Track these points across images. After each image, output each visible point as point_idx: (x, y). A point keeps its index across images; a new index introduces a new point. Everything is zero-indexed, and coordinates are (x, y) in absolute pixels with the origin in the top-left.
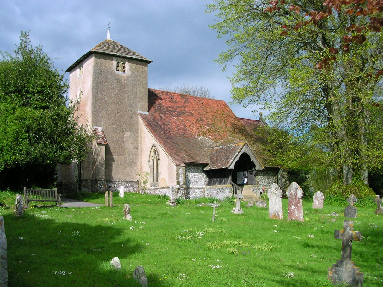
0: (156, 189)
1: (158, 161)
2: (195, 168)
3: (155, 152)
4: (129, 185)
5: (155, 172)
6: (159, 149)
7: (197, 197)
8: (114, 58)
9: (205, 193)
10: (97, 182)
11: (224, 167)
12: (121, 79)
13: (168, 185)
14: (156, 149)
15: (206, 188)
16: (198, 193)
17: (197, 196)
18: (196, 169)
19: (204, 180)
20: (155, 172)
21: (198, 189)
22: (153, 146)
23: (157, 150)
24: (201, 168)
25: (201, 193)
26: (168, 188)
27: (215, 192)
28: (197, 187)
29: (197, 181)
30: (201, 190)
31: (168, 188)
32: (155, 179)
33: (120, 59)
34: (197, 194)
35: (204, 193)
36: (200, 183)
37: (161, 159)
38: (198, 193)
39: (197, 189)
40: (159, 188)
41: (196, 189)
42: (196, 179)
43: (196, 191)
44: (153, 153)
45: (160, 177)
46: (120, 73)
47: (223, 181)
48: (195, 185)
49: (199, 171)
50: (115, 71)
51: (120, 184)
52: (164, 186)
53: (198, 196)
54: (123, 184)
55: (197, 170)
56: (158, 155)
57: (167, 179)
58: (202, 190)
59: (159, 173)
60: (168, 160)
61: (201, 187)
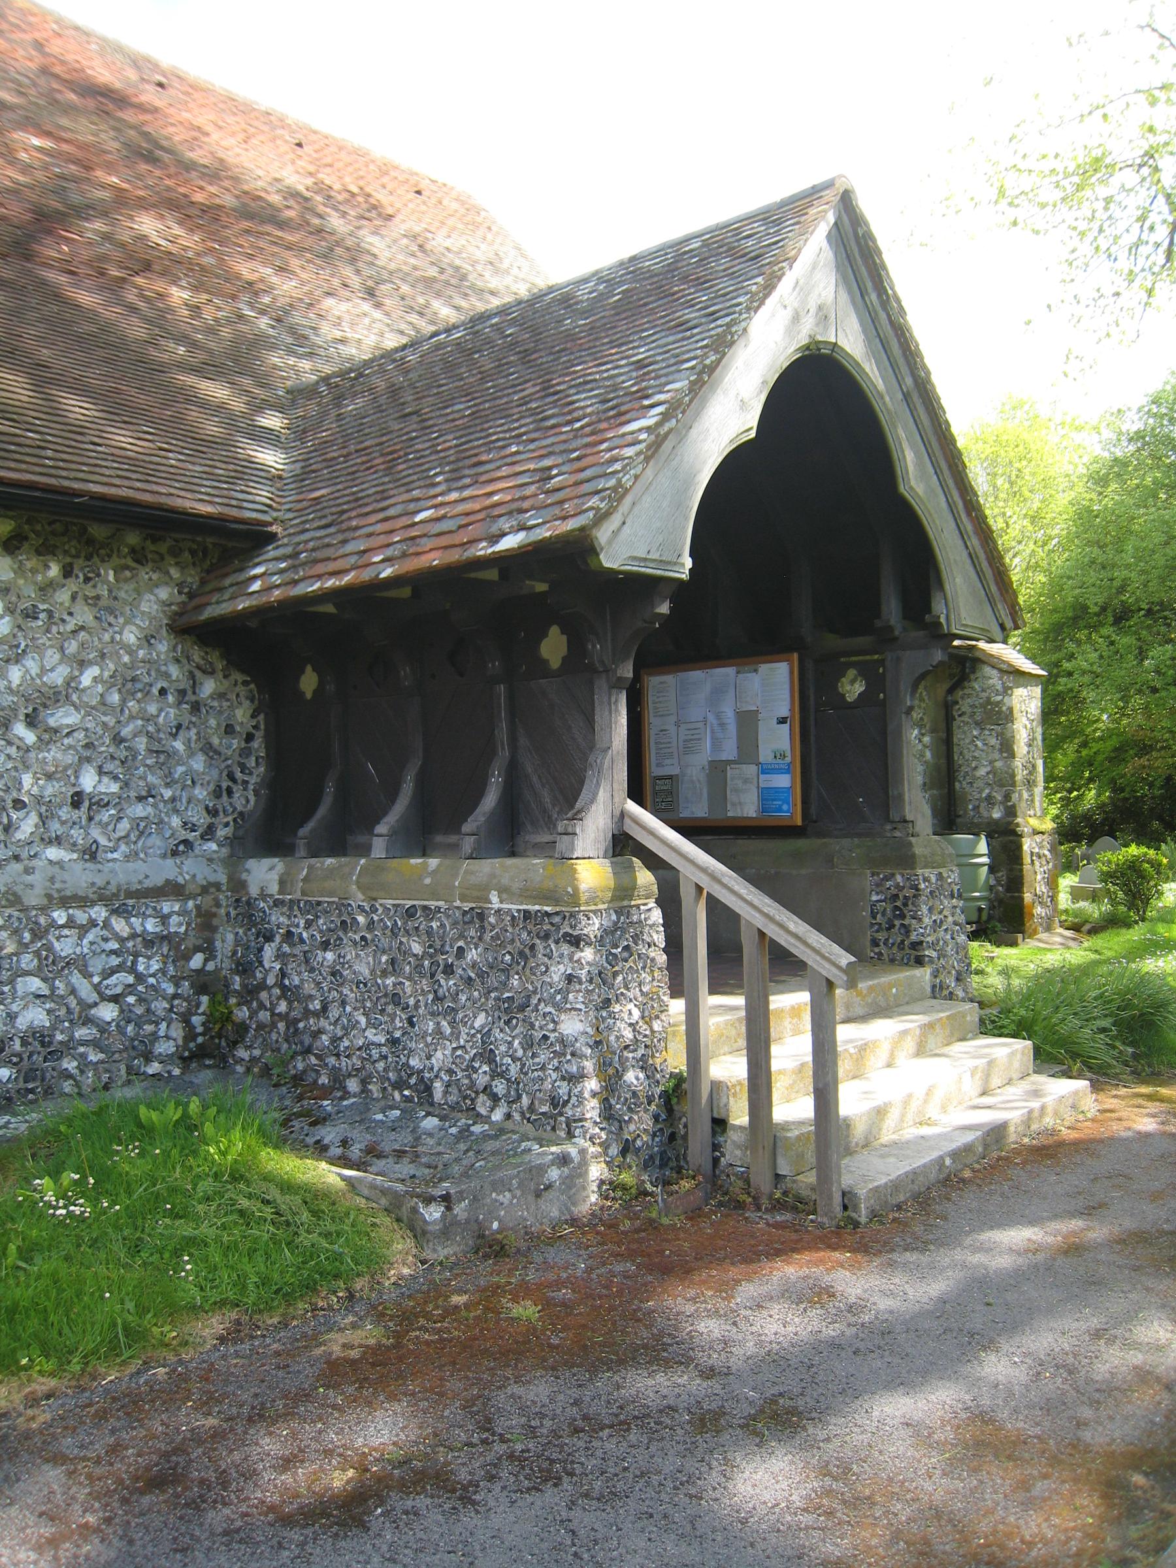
2: (46, 589)
7: (81, 1033)
9: (210, 953)
11: (510, 542)
15: (238, 885)
16: (97, 965)
17: (88, 1021)
18: (63, 596)
19: (198, 763)
21: (99, 913)
25: (150, 965)
27: (363, 970)
28: (81, 877)
29: (88, 781)
30: (151, 926)
34: (85, 990)
35: (197, 961)
36: (139, 810)
38: (97, 965)
39: (84, 902)
41: (60, 916)
42: (53, 755)
43: (65, 947)
47: (490, 800)
48: (53, 853)
49: (130, 637)
53: (108, 1012)
55: (84, 615)
58: (177, 925)
61: (167, 870)
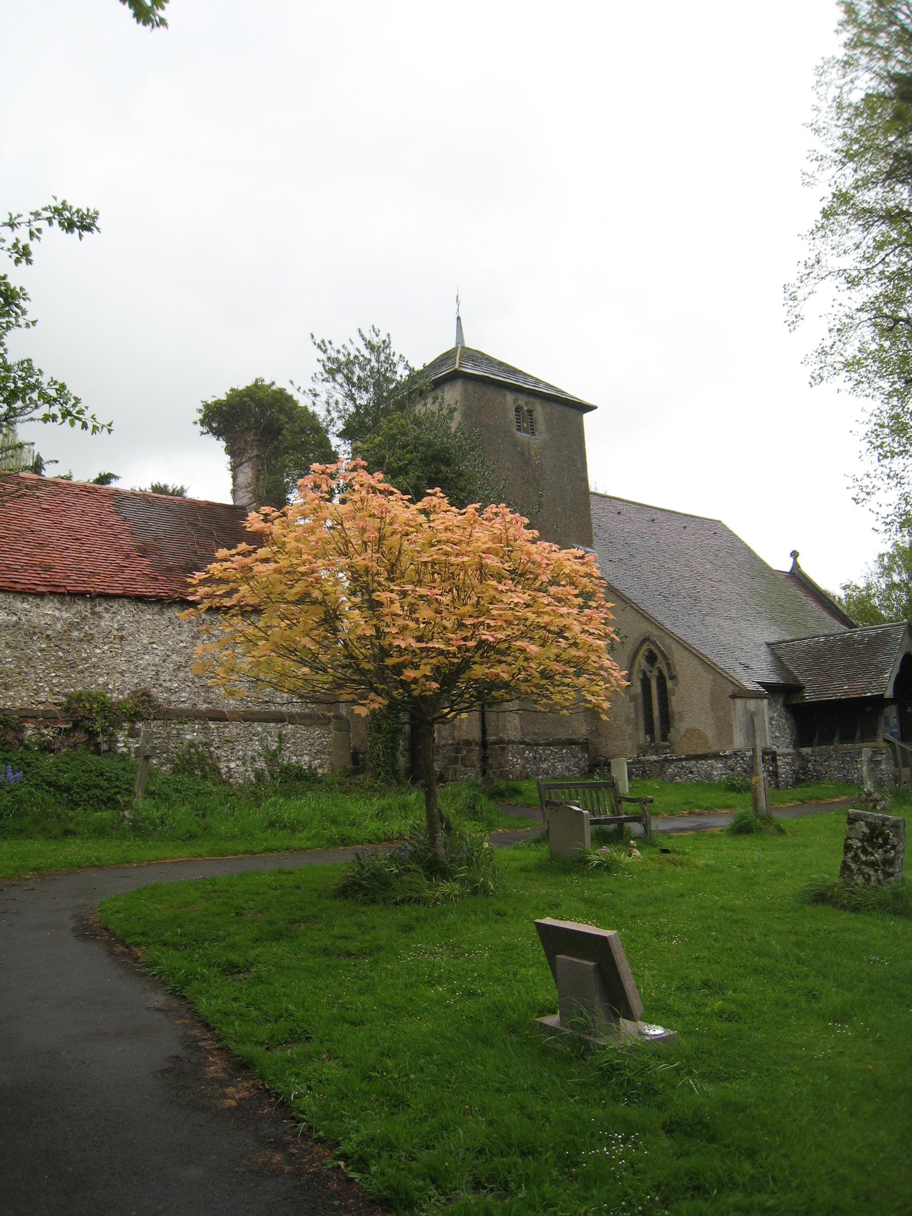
0: (666, 760)
1: (669, 684)
3: (651, 658)
4: (567, 752)
5: (656, 713)
6: (670, 648)
8: (510, 398)
10: (503, 749)
11: (869, 694)
12: (529, 453)
13: (714, 749)
14: (659, 648)
20: (656, 713)
22: (646, 640)
23: (662, 652)
24: (781, 700)
26: (716, 756)
31: (716, 756)
32: (658, 733)
33: (522, 400)
37: (678, 676)
40: (681, 760)
44: (641, 660)
45: (681, 727)
46: (523, 436)
50: (514, 429)
51: (547, 752)
52: (700, 752)
54: (555, 750)
56: (668, 665)
57: (710, 733)
59: (676, 717)
60: (711, 677)
